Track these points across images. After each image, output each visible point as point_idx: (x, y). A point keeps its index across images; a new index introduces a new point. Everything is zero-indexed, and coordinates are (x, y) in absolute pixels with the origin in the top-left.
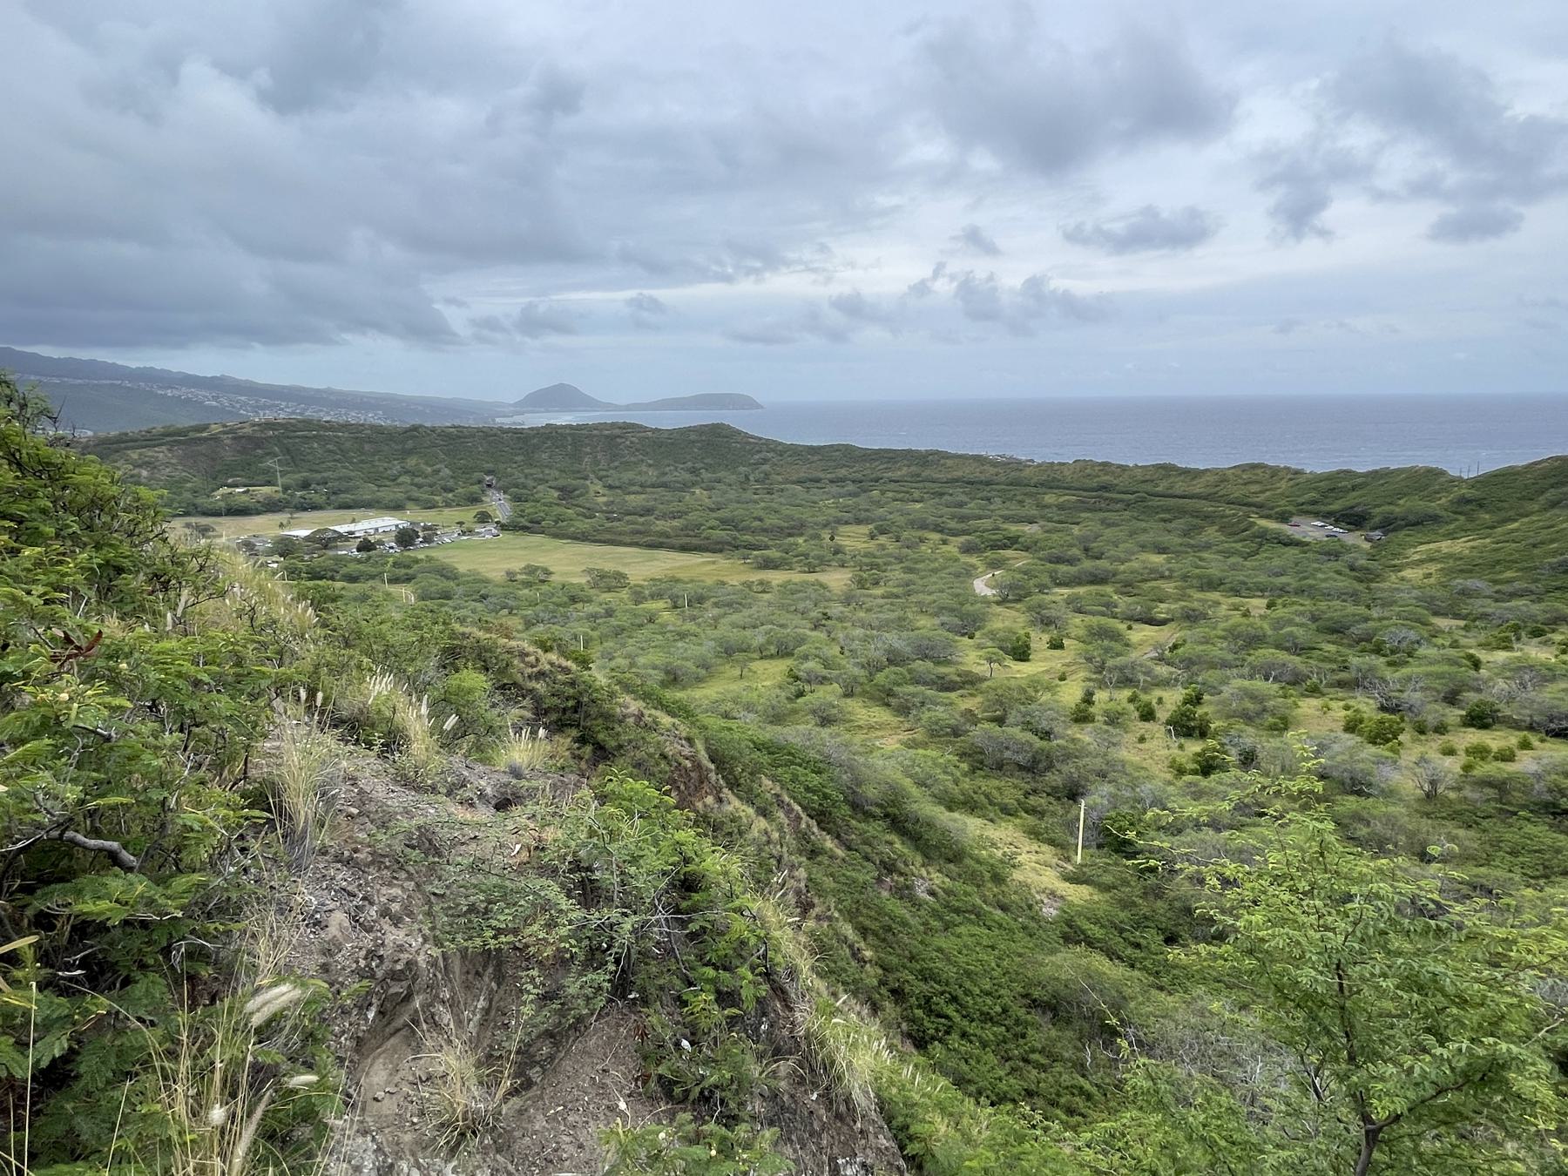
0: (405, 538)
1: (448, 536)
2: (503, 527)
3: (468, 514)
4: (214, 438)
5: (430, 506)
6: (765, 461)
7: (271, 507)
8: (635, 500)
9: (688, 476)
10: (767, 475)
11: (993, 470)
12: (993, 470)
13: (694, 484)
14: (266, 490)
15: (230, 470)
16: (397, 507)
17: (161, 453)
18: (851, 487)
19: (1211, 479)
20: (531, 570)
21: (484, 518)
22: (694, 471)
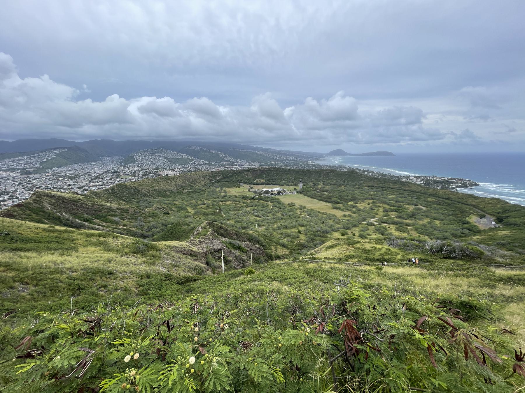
0: (279, 193)
1: (287, 192)
2: (297, 192)
3: (292, 188)
4: (257, 170)
5: (288, 185)
6: (362, 180)
7: (263, 184)
8: (327, 188)
9: (343, 183)
10: (361, 184)
11: (421, 189)
12: (421, 189)
13: (343, 185)
14: (263, 180)
15: (258, 176)
16: (282, 185)
17: (249, 173)
18: (380, 189)
19: (480, 200)
20: (292, 203)
21: (295, 189)
22: (344, 182)
